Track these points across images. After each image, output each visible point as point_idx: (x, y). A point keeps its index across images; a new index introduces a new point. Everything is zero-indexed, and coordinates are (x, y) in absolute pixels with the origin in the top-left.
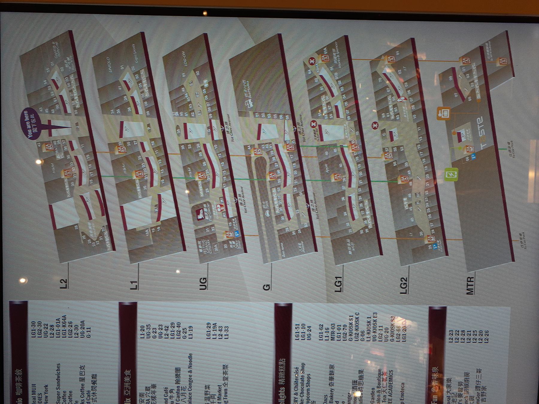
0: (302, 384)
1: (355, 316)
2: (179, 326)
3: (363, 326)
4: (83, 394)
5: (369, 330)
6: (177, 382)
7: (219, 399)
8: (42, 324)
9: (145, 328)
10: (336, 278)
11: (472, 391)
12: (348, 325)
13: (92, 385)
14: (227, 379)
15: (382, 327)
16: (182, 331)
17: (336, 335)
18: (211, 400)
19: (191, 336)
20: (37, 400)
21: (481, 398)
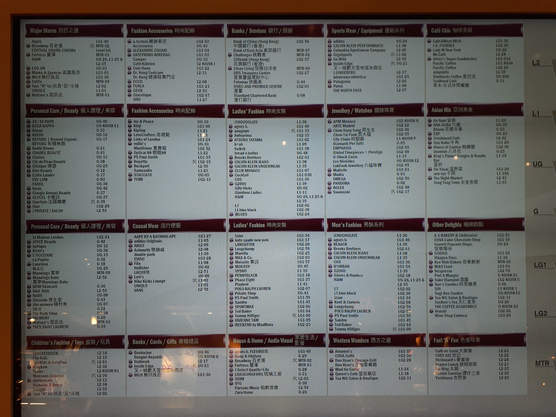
0: (463, 240)
1: (517, 278)
2: (506, 147)
3: (509, 284)
4: (454, 77)
5: (507, 288)
6: (464, 147)
7: (452, 178)
8: (506, 47)
9: (504, 122)
10: (545, 263)
11: (462, 369)
12: (510, 273)
13: (461, 84)
14: (467, 183)
15: (510, 298)
16: (502, 149)
17: (502, 264)
18: (451, 172)
19: (498, 156)
20: (449, 43)
21: (457, 376)
